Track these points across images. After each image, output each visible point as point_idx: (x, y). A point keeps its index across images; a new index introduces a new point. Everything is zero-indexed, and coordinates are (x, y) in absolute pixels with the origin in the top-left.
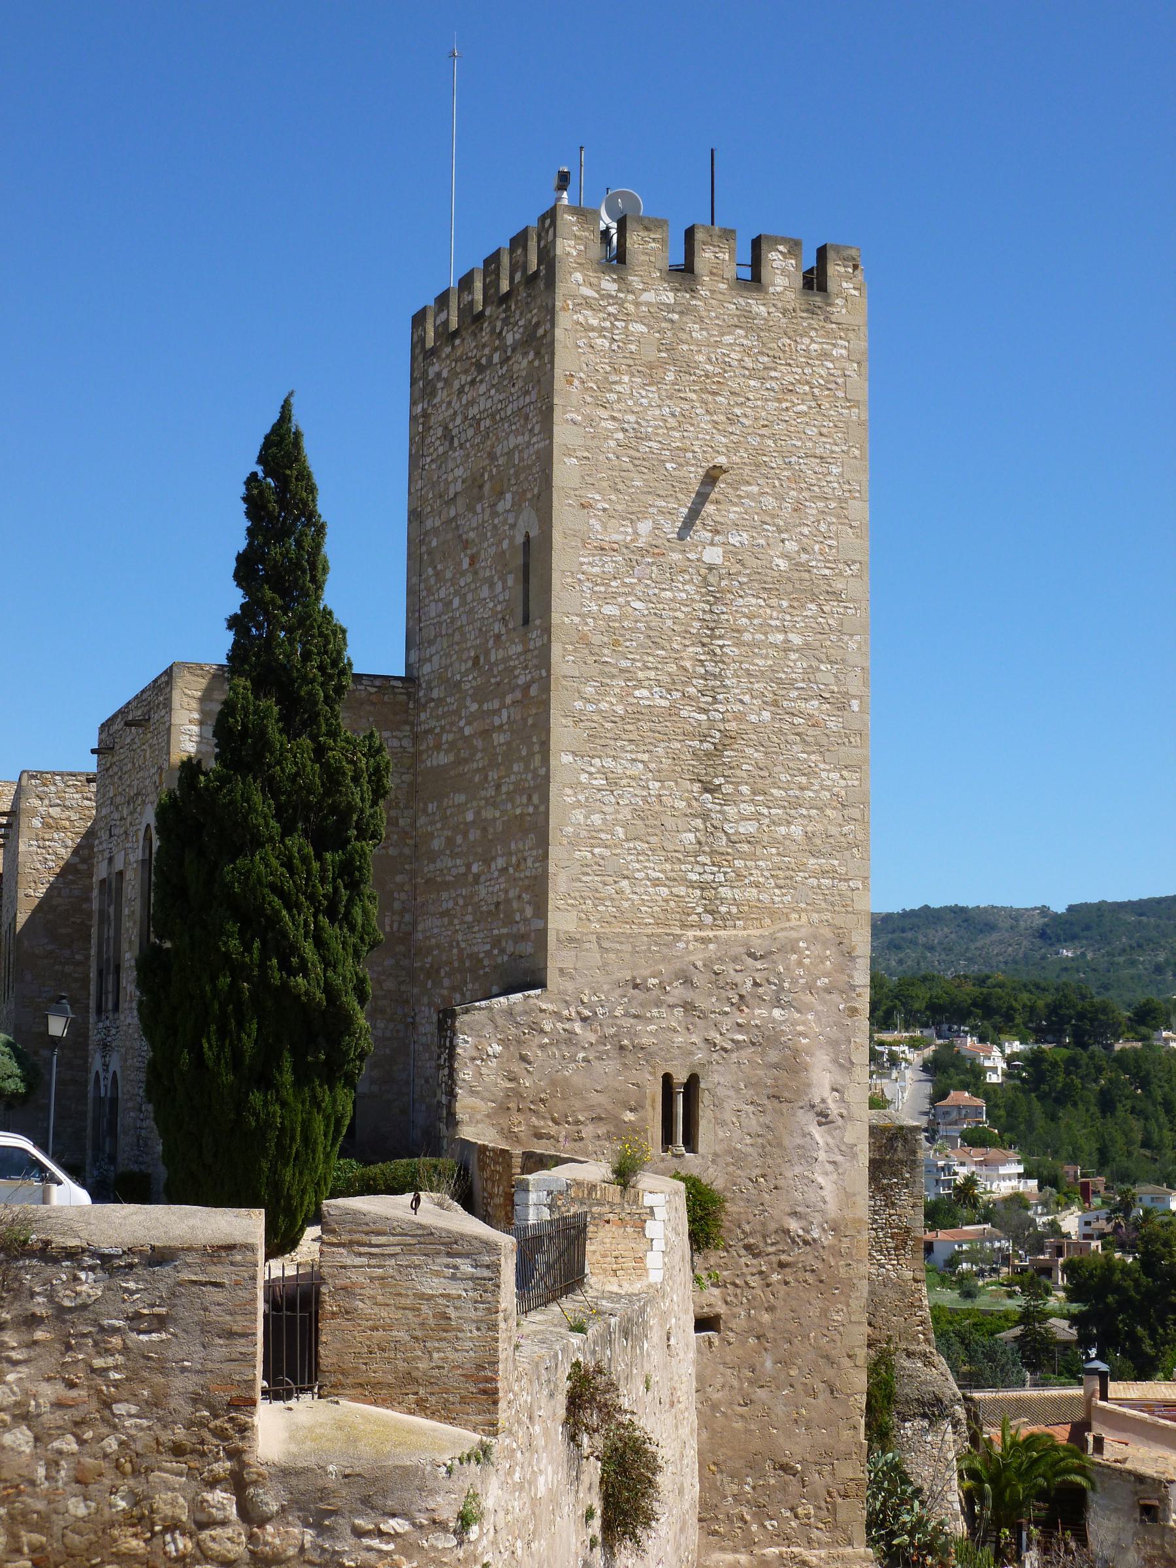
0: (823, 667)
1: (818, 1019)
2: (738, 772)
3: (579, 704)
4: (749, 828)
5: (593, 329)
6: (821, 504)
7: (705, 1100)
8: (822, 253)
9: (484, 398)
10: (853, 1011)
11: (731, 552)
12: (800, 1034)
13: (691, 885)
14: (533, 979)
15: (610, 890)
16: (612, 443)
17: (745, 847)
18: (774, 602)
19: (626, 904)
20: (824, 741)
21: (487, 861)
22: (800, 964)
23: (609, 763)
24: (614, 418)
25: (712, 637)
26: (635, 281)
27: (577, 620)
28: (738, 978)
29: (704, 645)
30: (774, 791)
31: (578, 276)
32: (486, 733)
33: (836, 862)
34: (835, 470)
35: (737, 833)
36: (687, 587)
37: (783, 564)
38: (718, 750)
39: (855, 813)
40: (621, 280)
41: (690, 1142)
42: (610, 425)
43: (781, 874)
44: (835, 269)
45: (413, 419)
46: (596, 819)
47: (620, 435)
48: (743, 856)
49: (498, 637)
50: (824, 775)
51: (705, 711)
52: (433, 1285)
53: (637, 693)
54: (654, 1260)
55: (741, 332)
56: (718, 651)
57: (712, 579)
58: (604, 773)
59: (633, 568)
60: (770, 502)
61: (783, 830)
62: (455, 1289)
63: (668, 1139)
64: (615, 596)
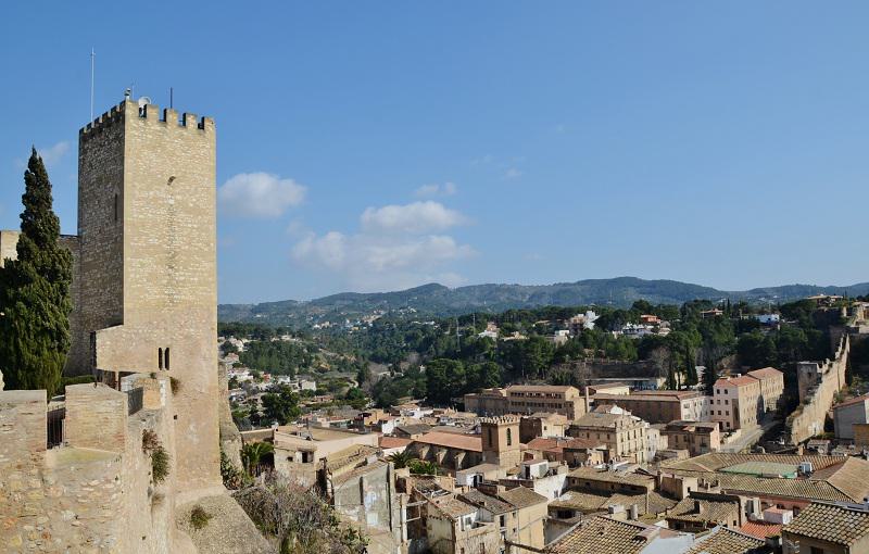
4: (182, 278)
8: (203, 119)
9: (102, 155)
10: (213, 329)
11: (176, 200)
14: (120, 322)
21: (104, 289)
31: (132, 121)
32: (103, 252)
38: (173, 257)
40: (145, 124)
41: (167, 366)
44: (206, 123)
45: (80, 160)
49: (107, 224)
52: (103, 409)
54: (163, 399)
60: (188, 188)
62: (109, 409)
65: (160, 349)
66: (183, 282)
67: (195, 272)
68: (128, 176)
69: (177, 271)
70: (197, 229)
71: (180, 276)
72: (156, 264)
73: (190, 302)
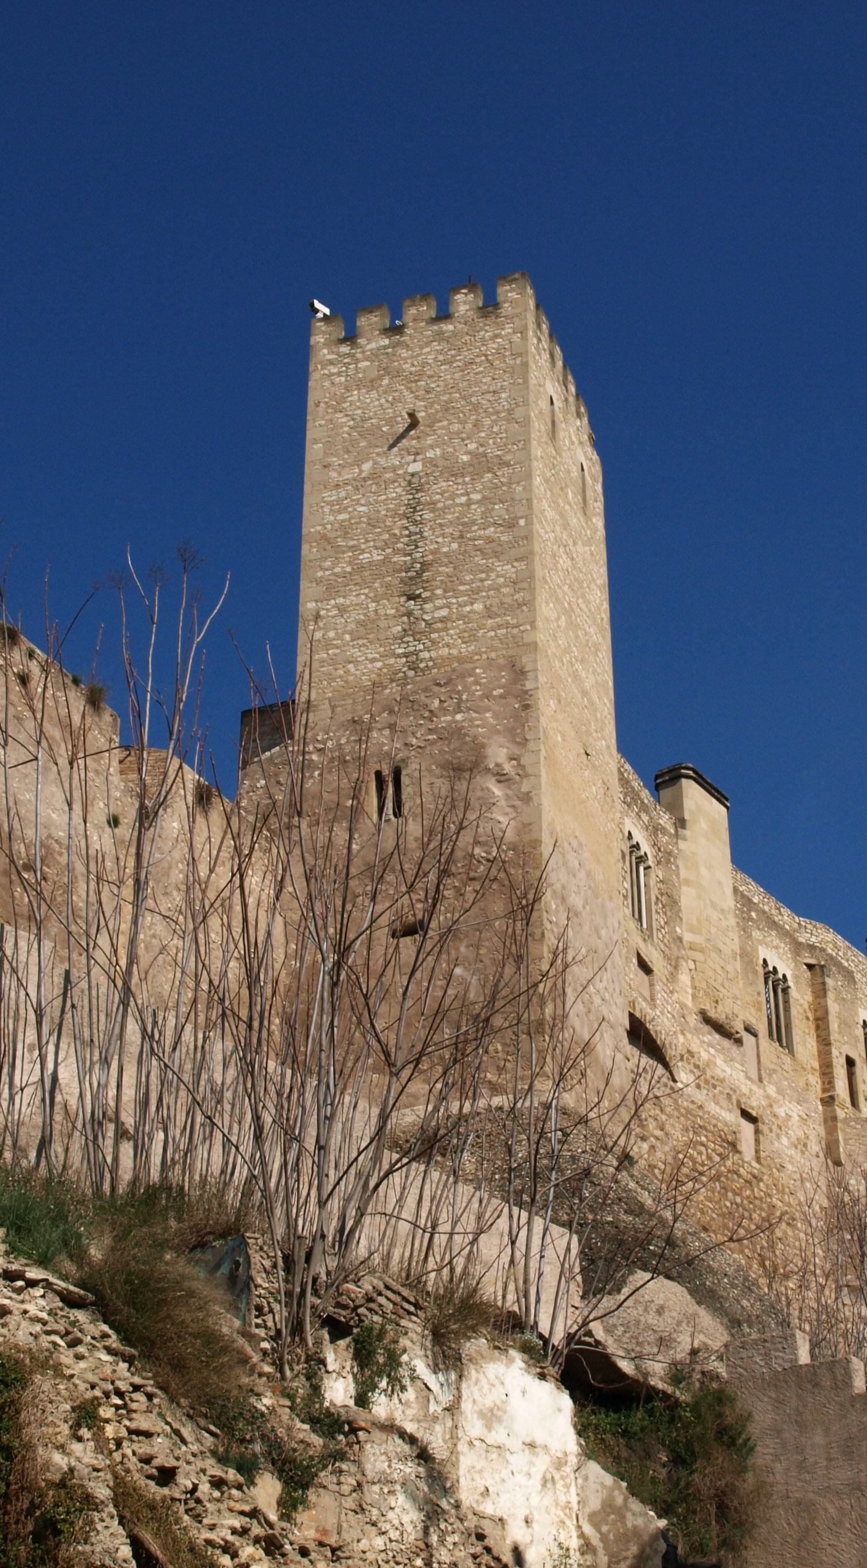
0: (496, 507)
1: (496, 716)
2: (434, 583)
3: (320, 574)
4: (444, 612)
5: (333, 374)
6: (494, 417)
7: (405, 780)
11: (426, 461)
12: (478, 726)
13: (399, 656)
15: (341, 672)
16: (346, 429)
17: (439, 625)
18: (460, 480)
19: (351, 678)
20: (499, 549)
22: (476, 683)
23: (341, 600)
24: (347, 415)
25: (415, 511)
26: (361, 341)
27: (319, 528)
29: (408, 518)
30: (461, 588)
31: (325, 351)
33: (508, 618)
34: (503, 395)
35: (433, 618)
36: (397, 490)
37: (465, 458)
38: (419, 574)
39: (525, 585)
41: (398, 811)
42: (344, 420)
43: (466, 635)
46: (331, 634)
47: (352, 423)
48: (437, 631)
50: (499, 569)
51: (410, 555)
53: (361, 557)
55: (435, 343)
56: (419, 518)
57: (415, 480)
58: (337, 606)
59: (358, 490)
61: (468, 609)
64: (346, 508)
65: (378, 774)
66: (442, 620)
67: (479, 590)
68: (314, 450)
69: (426, 601)
70: (478, 502)
71: (435, 610)
72: (376, 600)
73: (460, 660)
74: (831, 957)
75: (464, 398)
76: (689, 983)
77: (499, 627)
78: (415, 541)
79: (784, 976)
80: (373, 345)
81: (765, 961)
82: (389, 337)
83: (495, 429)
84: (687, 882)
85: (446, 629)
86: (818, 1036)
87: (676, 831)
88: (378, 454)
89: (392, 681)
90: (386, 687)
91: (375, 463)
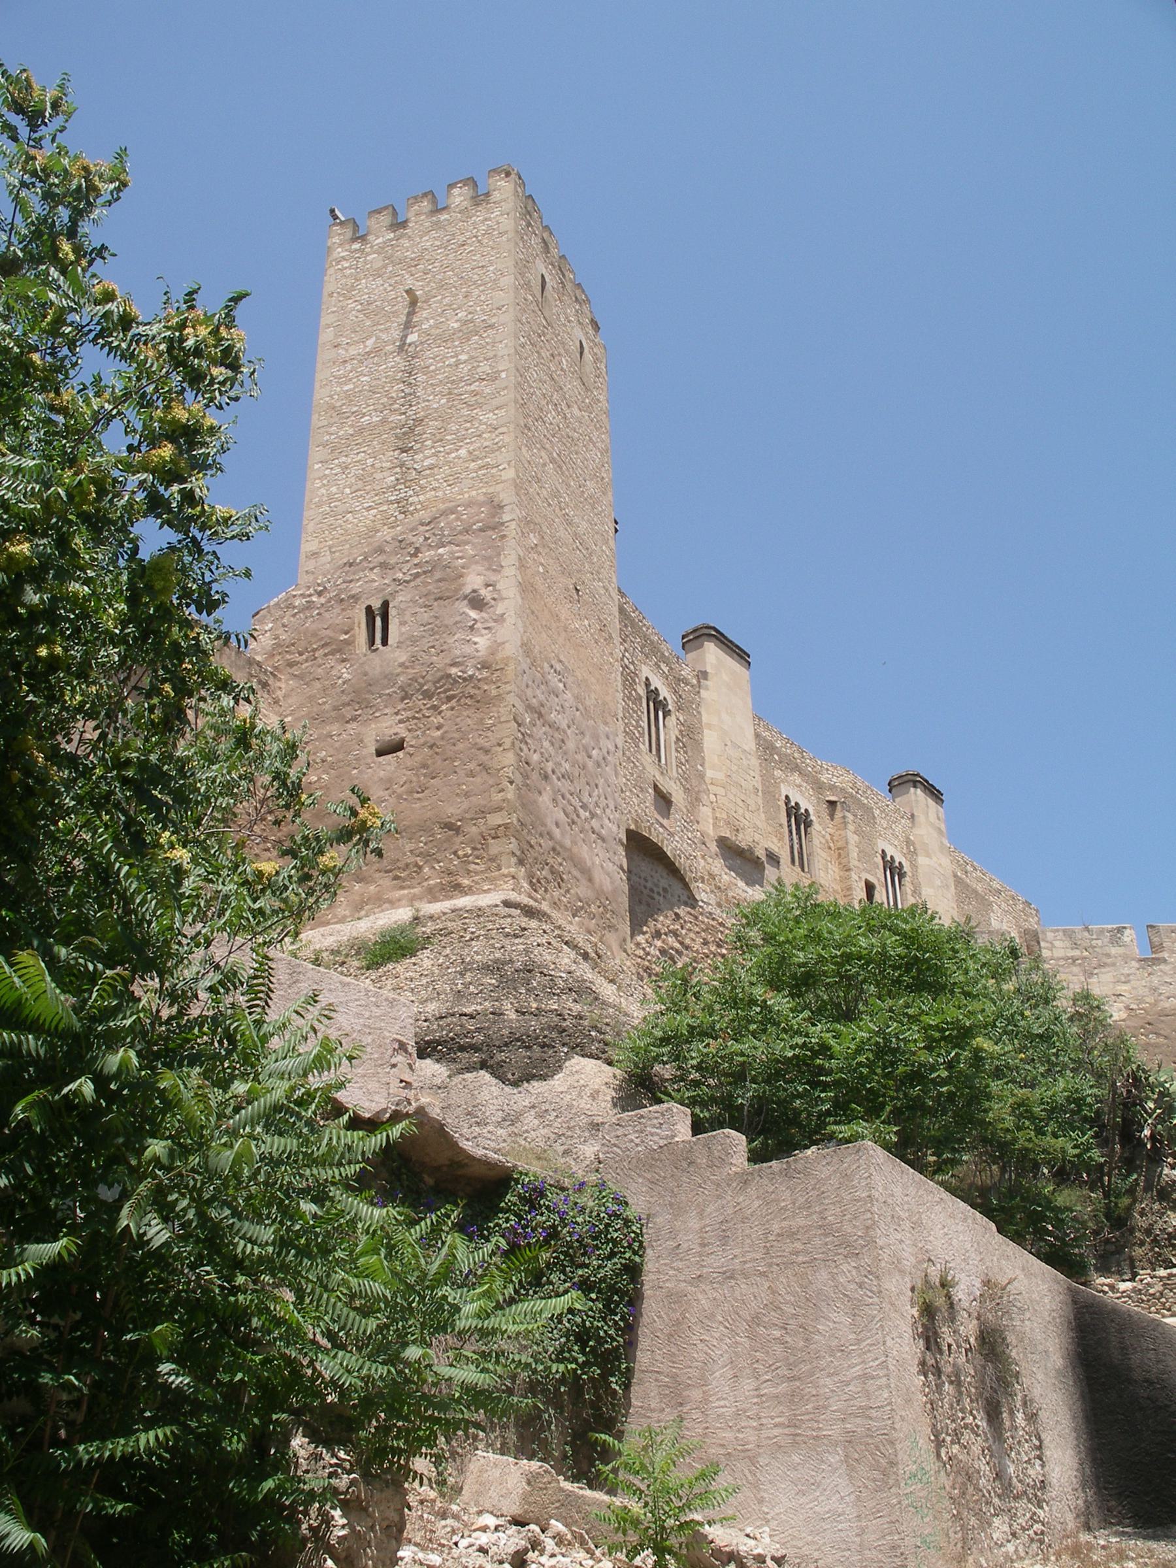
7: (392, 612)
13: (392, 503)
17: (428, 472)
28: (414, 539)
30: (448, 437)
34: (491, 268)
61: (453, 455)
63: (372, 641)
65: (369, 609)
71: (424, 459)
74: (852, 796)
75: (456, 275)
76: (710, 814)
77: (481, 468)
78: (409, 399)
79: (806, 810)
80: (380, 240)
81: (787, 797)
82: (394, 232)
83: (483, 298)
84: (710, 726)
85: (433, 475)
86: (840, 863)
87: (699, 682)
88: (381, 331)
89: (385, 524)
90: (378, 531)
91: (378, 338)
